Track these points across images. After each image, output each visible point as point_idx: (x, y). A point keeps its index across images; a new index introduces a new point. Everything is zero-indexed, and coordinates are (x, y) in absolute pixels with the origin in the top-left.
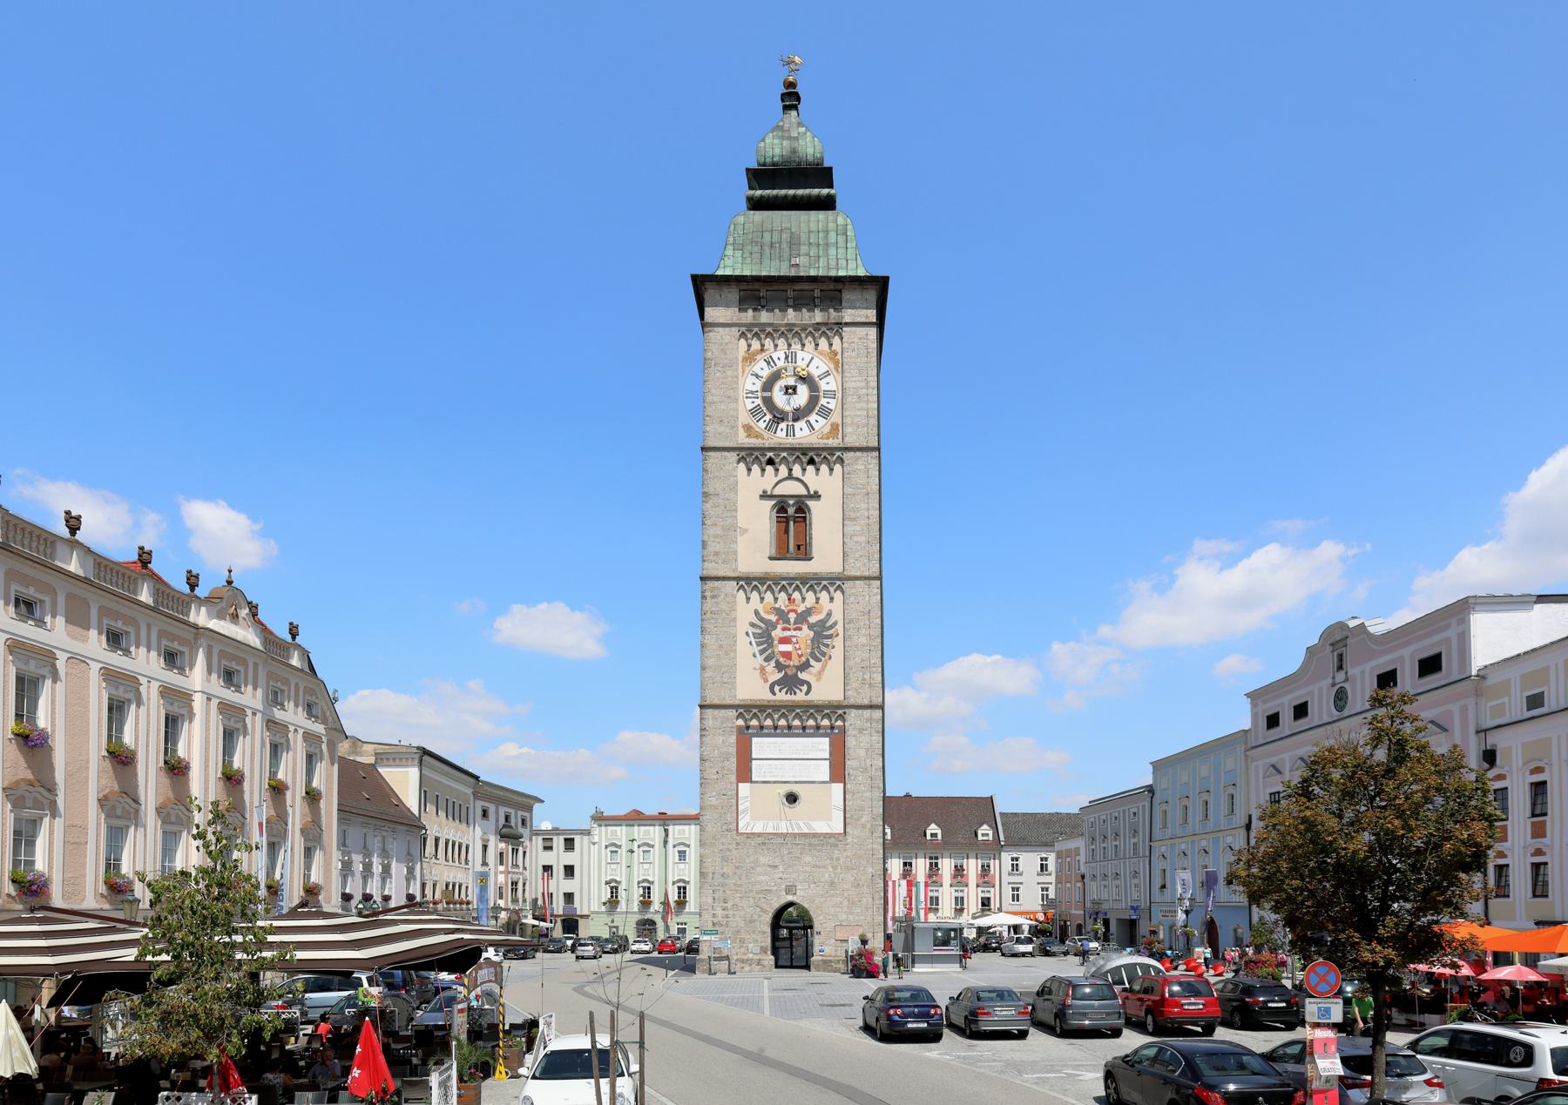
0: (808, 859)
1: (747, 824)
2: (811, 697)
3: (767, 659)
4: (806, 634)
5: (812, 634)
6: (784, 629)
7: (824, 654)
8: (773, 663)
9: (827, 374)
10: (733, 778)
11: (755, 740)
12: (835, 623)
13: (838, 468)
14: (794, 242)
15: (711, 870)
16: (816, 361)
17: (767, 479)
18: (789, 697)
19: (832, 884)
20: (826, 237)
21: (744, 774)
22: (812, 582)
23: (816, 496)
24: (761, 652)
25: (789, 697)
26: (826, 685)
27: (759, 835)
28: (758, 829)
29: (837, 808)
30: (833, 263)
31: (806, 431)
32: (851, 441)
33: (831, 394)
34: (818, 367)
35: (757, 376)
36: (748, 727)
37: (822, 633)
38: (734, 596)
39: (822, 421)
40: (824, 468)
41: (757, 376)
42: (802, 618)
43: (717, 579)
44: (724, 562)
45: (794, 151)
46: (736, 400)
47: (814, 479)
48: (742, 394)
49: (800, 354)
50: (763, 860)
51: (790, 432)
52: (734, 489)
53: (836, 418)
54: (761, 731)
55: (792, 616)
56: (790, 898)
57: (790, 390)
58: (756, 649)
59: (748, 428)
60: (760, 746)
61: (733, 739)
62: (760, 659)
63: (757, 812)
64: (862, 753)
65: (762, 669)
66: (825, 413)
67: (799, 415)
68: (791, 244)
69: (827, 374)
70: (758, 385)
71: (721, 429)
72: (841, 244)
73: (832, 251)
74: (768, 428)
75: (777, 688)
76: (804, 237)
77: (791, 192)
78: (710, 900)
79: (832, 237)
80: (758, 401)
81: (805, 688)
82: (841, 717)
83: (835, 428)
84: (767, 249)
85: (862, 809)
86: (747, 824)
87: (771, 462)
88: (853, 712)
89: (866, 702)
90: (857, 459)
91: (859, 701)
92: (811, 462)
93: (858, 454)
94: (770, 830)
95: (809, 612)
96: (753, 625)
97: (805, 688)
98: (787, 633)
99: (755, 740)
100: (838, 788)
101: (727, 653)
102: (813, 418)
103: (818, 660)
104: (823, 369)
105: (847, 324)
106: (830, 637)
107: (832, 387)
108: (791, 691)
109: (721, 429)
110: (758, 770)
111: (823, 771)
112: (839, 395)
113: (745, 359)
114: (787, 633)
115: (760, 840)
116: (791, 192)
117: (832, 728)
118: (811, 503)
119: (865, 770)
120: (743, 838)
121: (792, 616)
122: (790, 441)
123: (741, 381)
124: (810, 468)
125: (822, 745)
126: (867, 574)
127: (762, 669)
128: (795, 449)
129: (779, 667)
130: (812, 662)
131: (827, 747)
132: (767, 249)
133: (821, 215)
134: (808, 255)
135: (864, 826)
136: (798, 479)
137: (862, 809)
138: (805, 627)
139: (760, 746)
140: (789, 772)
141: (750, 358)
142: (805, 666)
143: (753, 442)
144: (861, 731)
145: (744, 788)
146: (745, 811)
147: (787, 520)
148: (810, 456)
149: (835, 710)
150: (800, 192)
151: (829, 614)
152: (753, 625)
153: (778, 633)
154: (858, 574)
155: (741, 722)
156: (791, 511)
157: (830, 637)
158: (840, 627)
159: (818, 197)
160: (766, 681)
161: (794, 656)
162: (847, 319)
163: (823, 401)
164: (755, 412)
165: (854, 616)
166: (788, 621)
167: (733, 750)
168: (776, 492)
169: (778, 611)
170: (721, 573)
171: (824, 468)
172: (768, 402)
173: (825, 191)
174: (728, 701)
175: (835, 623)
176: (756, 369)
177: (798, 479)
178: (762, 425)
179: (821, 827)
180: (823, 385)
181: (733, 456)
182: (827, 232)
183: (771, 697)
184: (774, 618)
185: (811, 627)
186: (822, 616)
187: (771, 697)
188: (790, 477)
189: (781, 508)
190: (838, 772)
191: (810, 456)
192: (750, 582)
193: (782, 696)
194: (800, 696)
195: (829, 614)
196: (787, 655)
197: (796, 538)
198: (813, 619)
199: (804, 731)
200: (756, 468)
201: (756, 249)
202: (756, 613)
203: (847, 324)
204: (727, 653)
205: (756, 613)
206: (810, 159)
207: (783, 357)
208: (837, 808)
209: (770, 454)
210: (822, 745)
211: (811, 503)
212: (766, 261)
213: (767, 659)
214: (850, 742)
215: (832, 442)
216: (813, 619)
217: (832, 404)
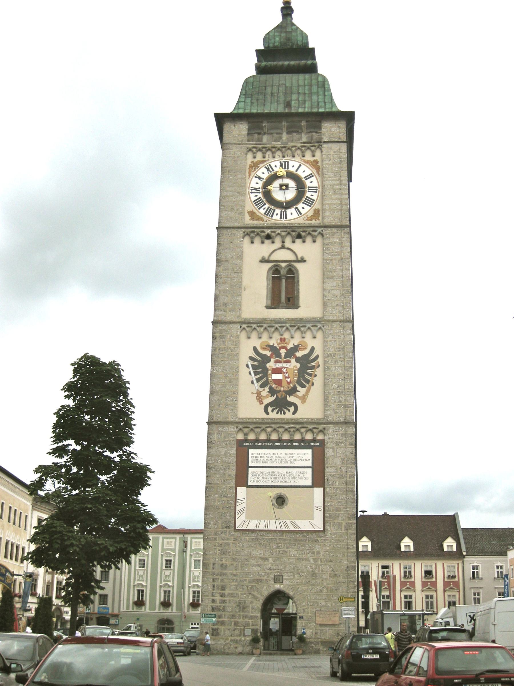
0: (293, 552)
1: (243, 522)
2: (297, 416)
3: (262, 386)
4: (294, 365)
5: (298, 365)
6: (276, 362)
7: (308, 381)
8: (267, 389)
9: (311, 176)
10: (233, 483)
11: (251, 451)
12: (317, 357)
13: (319, 240)
14: (288, 92)
15: (212, 561)
16: (303, 168)
17: (265, 249)
18: (279, 416)
19: (314, 575)
20: (310, 89)
21: (242, 480)
22: (299, 325)
23: (303, 261)
24: (258, 380)
25: (279, 416)
26: (310, 406)
27: (253, 531)
28: (252, 527)
29: (317, 508)
30: (315, 104)
31: (295, 215)
32: (328, 221)
33: (313, 189)
34: (304, 171)
35: (259, 178)
36: (246, 440)
37: (306, 363)
38: (238, 336)
39: (307, 208)
40: (309, 239)
41: (259, 178)
42: (291, 353)
43: (225, 323)
44: (231, 311)
45: (289, 39)
46: (245, 194)
47: (301, 248)
48: (249, 190)
49: (291, 163)
50: (255, 553)
51: (283, 216)
52: (240, 257)
53: (317, 206)
54: (257, 444)
55: (283, 352)
56: (278, 586)
57: (284, 187)
58: (254, 378)
59: (252, 214)
60: (255, 456)
61: (233, 451)
62: (257, 385)
63: (251, 514)
64: (339, 462)
65: (259, 393)
66: (309, 202)
67: (289, 205)
68: (285, 94)
69: (311, 176)
70: (260, 184)
71: (232, 214)
72: (321, 93)
73: (315, 98)
74: (267, 213)
75: (270, 409)
76: (294, 90)
77: (286, 63)
78: (210, 588)
79: (315, 89)
80: (260, 195)
81: (292, 409)
82: (322, 431)
83: (317, 213)
84: (268, 97)
85: (338, 510)
86: (243, 522)
87: (268, 237)
88: (331, 428)
89: (342, 419)
90: (334, 234)
91: (336, 420)
92: (299, 236)
93: (334, 230)
94: (261, 528)
95: (296, 348)
96: (251, 358)
97: (292, 409)
98: (280, 365)
99: (251, 451)
100: (318, 492)
101: (230, 381)
102: (300, 206)
103: (303, 386)
104: (308, 172)
105: (325, 142)
106: (313, 368)
107: (315, 184)
108: (281, 411)
109: (232, 214)
110: (254, 477)
111: (306, 478)
112: (320, 190)
113: (251, 167)
114: (280, 365)
115: (253, 535)
116: (286, 63)
117: (314, 440)
118: (298, 265)
119: (341, 477)
120: (239, 534)
121: (283, 352)
122: (283, 221)
123: (248, 181)
124: (298, 241)
125: (306, 456)
126: (342, 318)
127: (259, 393)
128: (286, 227)
129: (272, 392)
130: (299, 388)
131: (310, 457)
132: (268, 97)
133: (307, 76)
134: (298, 99)
135: (340, 524)
136: (288, 249)
137: (338, 510)
138: (293, 360)
139: (255, 456)
140: (279, 478)
141: (255, 166)
142: (293, 391)
143: (255, 223)
144: (338, 444)
145: (241, 492)
146: (242, 510)
147: (279, 278)
148: (299, 233)
149: (317, 425)
150: (292, 63)
151: (313, 349)
152: (251, 358)
153: (271, 365)
154: (335, 318)
155: (240, 436)
156: (283, 272)
157: (313, 368)
158: (320, 360)
159: (306, 65)
160: (261, 403)
161: (284, 384)
162: (325, 139)
163: (308, 194)
164: (257, 202)
165: (332, 351)
166: (279, 355)
167: (234, 459)
168: (272, 258)
169: (272, 348)
170: (228, 319)
171: (309, 239)
172: (268, 195)
173: (310, 62)
174: (230, 419)
175: (317, 357)
176: (259, 173)
177: (288, 249)
178: (262, 211)
179: (304, 525)
180: (308, 183)
181: (240, 233)
182: (311, 86)
183: (264, 416)
184: (268, 353)
185: (298, 360)
186: (306, 352)
187: (264, 416)
188: (283, 247)
189: (276, 270)
190: (319, 479)
191: (299, 233)
192: (251, 325)
193: (274, 415)
194: (288, 415)
195: (313, 349)
196: (279, 382)
197: (287, 293)
198: (299, 354)
199: (291, 444)
200: (257, 240)
201: (261, 97)
202: (255, 349)
203: (325, 142)
204: (230, 381)
205: (255, 349)
206: (300, 43)
207: (278, 164)
208: (317, 508)
209: (268, 231)
210: (306, 456)
211: (298, 265)
212: (268, 104)
213: (262, 386)
214: (329, 452)
215: (313, 222)
216: (299, 354)
217: (315, 196)
